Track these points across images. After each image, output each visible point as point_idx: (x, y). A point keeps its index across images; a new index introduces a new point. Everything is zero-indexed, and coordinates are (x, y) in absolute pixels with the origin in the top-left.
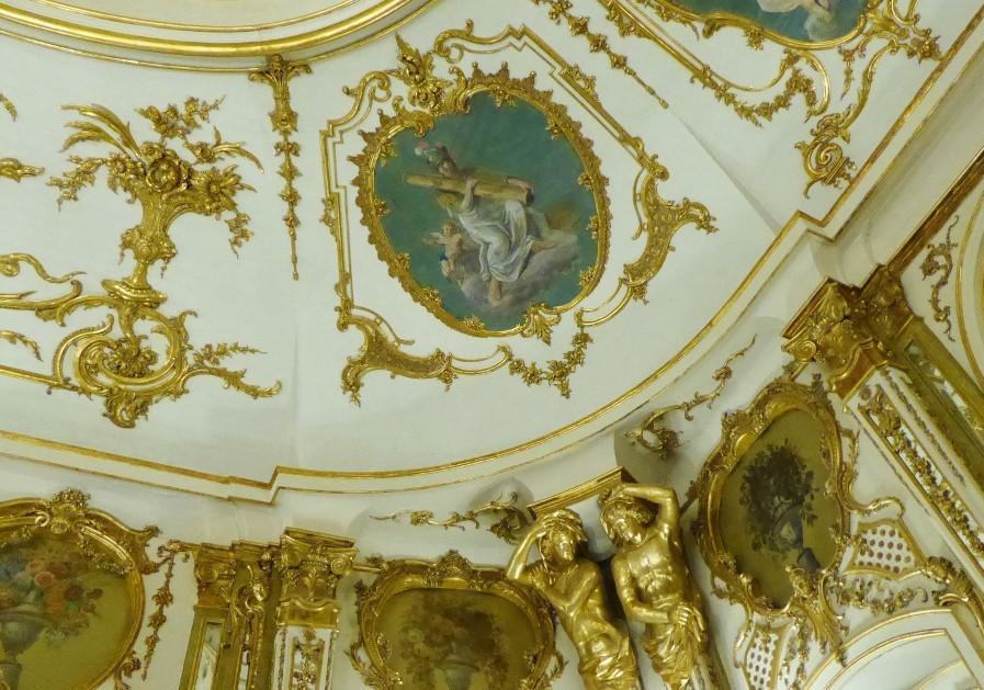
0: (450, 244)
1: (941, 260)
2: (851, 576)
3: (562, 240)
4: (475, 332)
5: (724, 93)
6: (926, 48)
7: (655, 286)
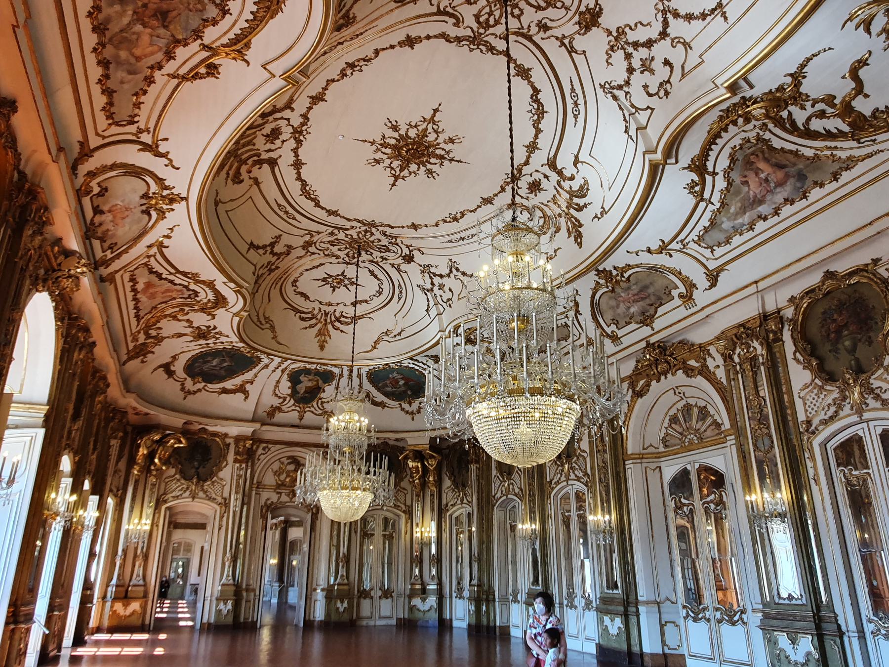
0: (209, 359)
1: (267, 450)
2: (205, 487)
3: (223, 372)
5: (276, 386)
7: (223, 395)
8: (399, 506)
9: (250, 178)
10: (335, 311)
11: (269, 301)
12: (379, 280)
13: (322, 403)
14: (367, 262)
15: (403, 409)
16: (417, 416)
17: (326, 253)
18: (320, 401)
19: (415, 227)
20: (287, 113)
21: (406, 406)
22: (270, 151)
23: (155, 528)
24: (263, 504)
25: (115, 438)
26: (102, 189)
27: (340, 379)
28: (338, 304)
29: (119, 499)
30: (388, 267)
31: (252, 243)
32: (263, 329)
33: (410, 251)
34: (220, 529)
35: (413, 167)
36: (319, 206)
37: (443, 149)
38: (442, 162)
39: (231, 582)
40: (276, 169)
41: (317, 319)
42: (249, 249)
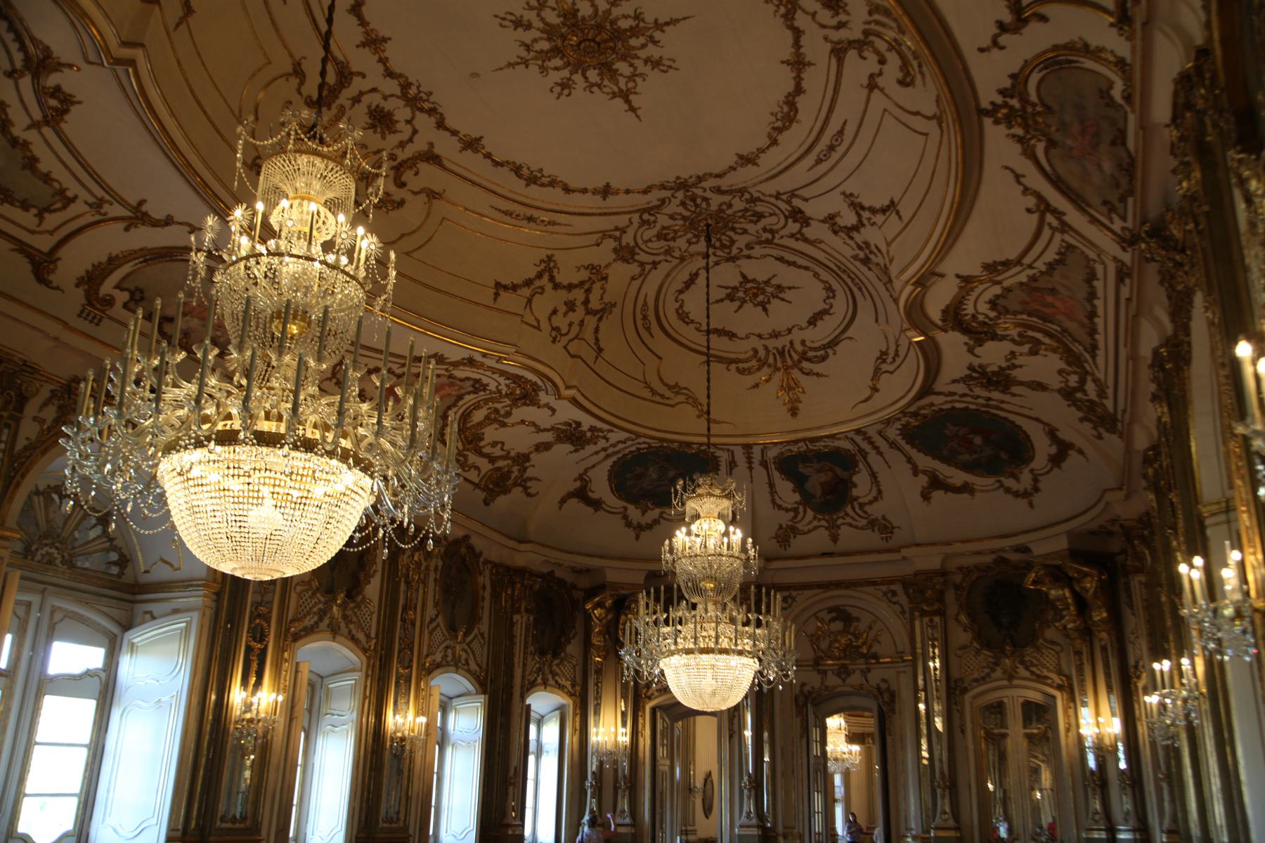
1: (790, 601)
4: (620, 498)
6: (835, 539)
8: (1047, 678)
9: (415, 193)
10: (791, 343)
11: (660, 358)
12: (807, 268)
13: (862, 506)
14: (757, 247)
15: (1008, 490)
16: (1037, 499)
17: (677, 254)
18: (855, 503)
19: (747, 160)
20: (357, 85)
21: (1009, 482)
22: (402, 145)
23: (641, 740)
24: (798, 692)
25: (519, 611)
26: (132, 293)
27: (865, 458)
28: (789, 331)
29: (578, 700)
30: (786, 242)
31: (498, 285)
32: (673, 406)
33: (789, 202)
34: (731, 737)
35: (623, 67)
36: (573, 191)
37: (626, 17)
38: (651, 37)
39: (754, 821)
40: (446, 163)
41: (770, 366)
42: (497, 295)
